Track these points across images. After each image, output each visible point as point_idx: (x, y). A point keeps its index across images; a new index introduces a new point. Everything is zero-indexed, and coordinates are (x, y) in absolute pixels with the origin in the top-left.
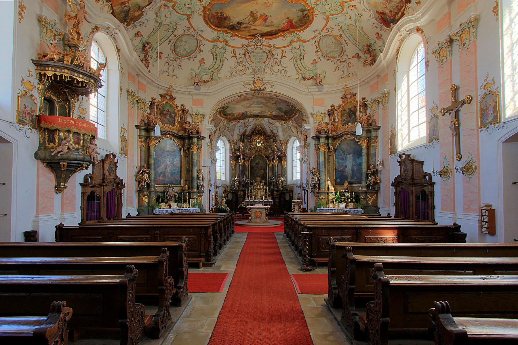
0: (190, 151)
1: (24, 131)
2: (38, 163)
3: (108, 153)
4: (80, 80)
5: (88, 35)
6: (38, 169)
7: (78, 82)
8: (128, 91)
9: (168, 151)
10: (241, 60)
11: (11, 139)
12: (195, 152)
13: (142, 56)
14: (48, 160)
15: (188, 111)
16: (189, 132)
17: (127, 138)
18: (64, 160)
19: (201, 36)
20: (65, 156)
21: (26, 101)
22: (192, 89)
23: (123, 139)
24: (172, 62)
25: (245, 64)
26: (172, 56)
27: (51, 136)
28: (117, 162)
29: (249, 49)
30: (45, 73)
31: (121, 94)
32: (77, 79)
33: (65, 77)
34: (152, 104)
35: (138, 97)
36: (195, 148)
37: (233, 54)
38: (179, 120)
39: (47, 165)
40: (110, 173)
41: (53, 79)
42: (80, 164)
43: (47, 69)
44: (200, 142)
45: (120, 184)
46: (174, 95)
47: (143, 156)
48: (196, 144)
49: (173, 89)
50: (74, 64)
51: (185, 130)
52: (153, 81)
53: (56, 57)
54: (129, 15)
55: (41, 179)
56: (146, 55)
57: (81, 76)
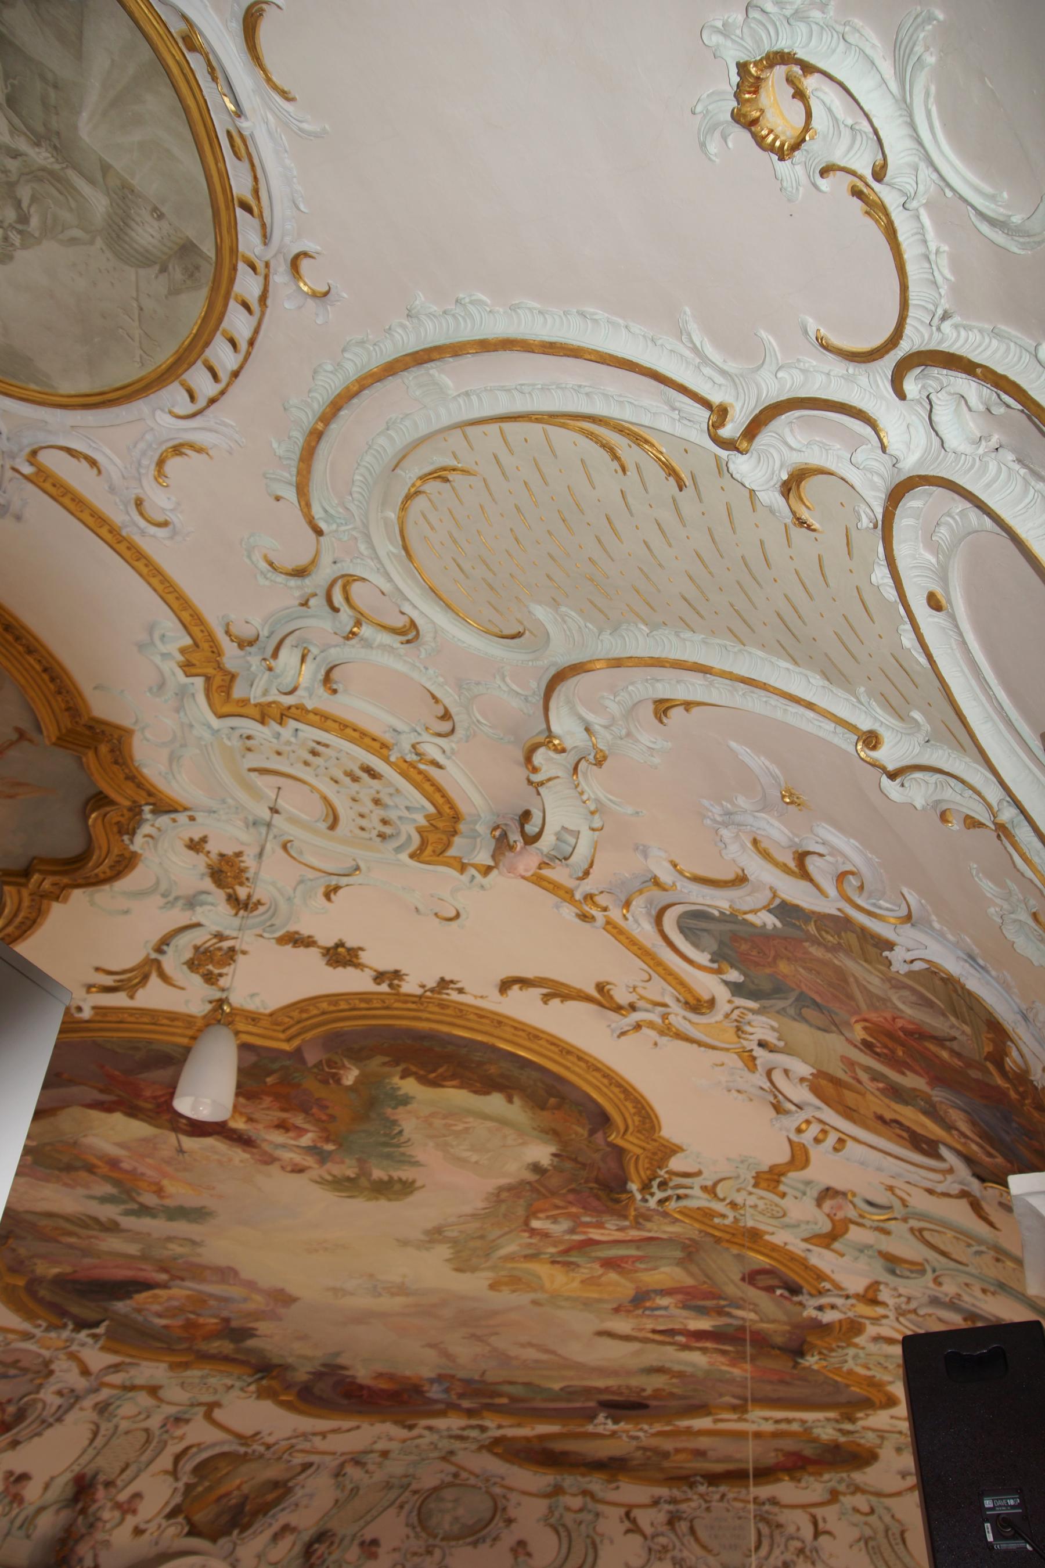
10: (662, 1540)
19: (503, 1486)
25: (676, 1553)
29: (683, 1507)
37: (627, 1524)
54: (247, 1508)
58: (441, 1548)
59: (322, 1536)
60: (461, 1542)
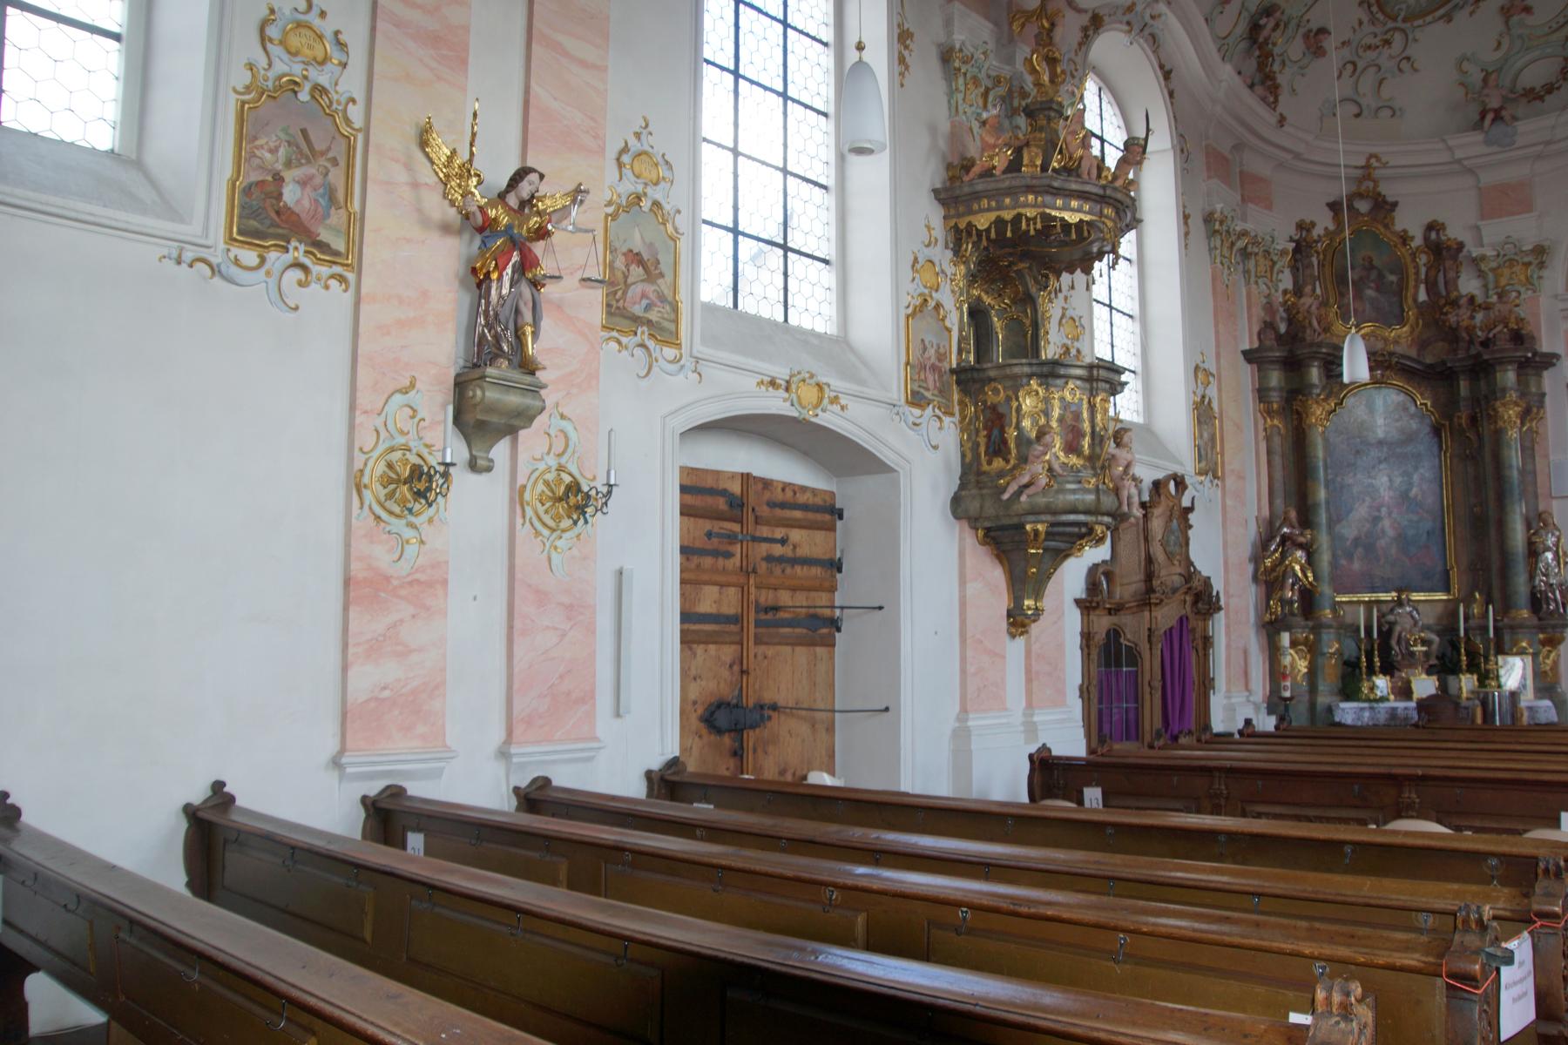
0: (1486, 429)
1: (924, 425)
2: (961, 531)
3: (1160, 475)
4: (1072, 218)
5: (1072, 55)
6: (962, 555)
7: (1066, 226)
8: (1208, 219)
9: (1381, 443)
11: (892, 456)
12: (1513, 434)
13: (1251, 65)
14: (988, 518)
15: (1461, 246)
16: (1471, 342)
17: (1215, 405)
18: (1035, 512)
20: (1042, 501)
21: (926, 329)
22: (1471, 145)
23: (1203, 413)
24: (1371, 55)
26: (1367, 28)
27: (996, 432)
28: (1191, 509)
30: (970, 224)
31: (1187, 234)
32: (1062, 219)
33: (1028, 220)
34: (1301, 249)
35: (1244, 233)
36: (1512, 413)
38: (1422, 296)
39: (986, 535)
40: (1170, 556)
41: (993, 235)
42: (1085, 524)
43: (976, 207)
44: (1532, 381)
45: (1203, 600)
46: (1389, 191)
47: (1278, 475)
48: (1514, 395)
49: (1385, 165)
50: (1054, 170)
51: (1452, 336)
52: (1297, 156)
53: (1000, 163)
55: (973, 588)
56: (1265, 59)
57: (1074, 204)
58: (1403, 31)
59: (1268, 11)
60: (1429, 18)
